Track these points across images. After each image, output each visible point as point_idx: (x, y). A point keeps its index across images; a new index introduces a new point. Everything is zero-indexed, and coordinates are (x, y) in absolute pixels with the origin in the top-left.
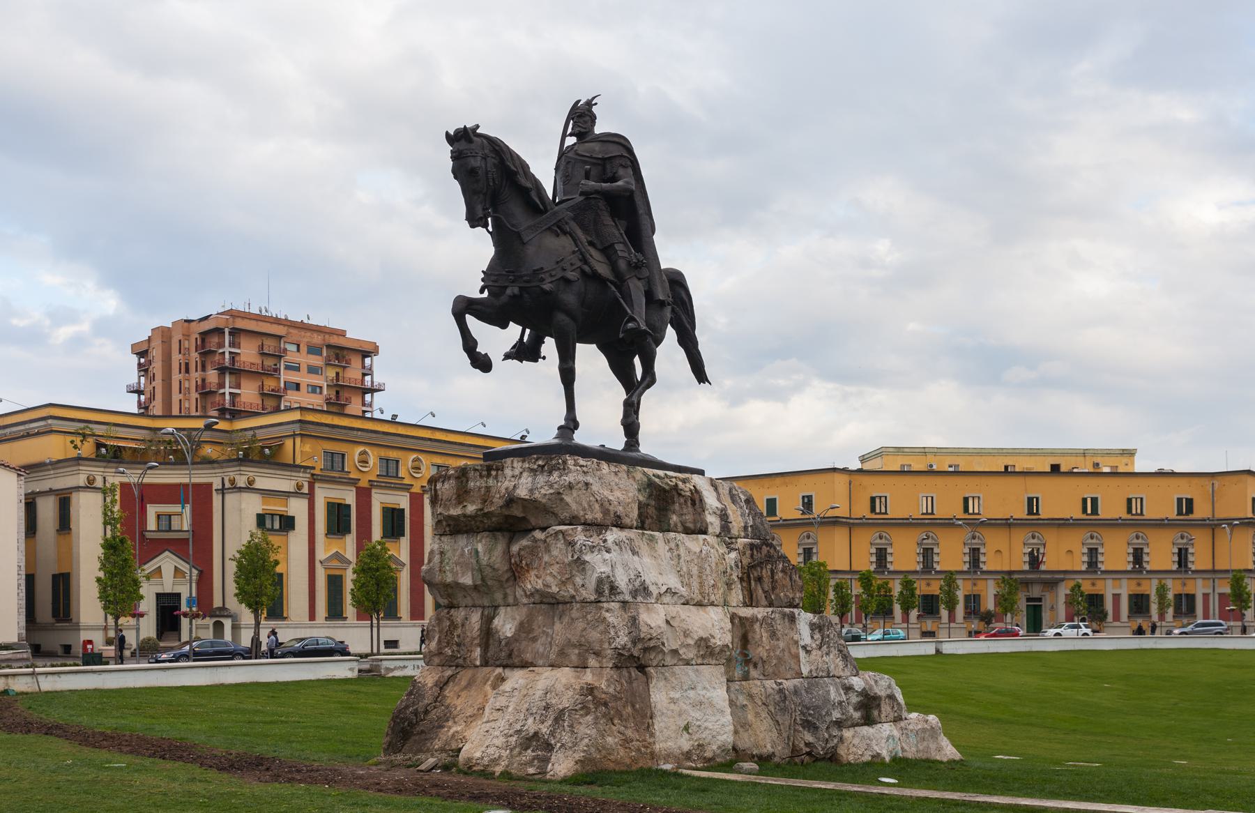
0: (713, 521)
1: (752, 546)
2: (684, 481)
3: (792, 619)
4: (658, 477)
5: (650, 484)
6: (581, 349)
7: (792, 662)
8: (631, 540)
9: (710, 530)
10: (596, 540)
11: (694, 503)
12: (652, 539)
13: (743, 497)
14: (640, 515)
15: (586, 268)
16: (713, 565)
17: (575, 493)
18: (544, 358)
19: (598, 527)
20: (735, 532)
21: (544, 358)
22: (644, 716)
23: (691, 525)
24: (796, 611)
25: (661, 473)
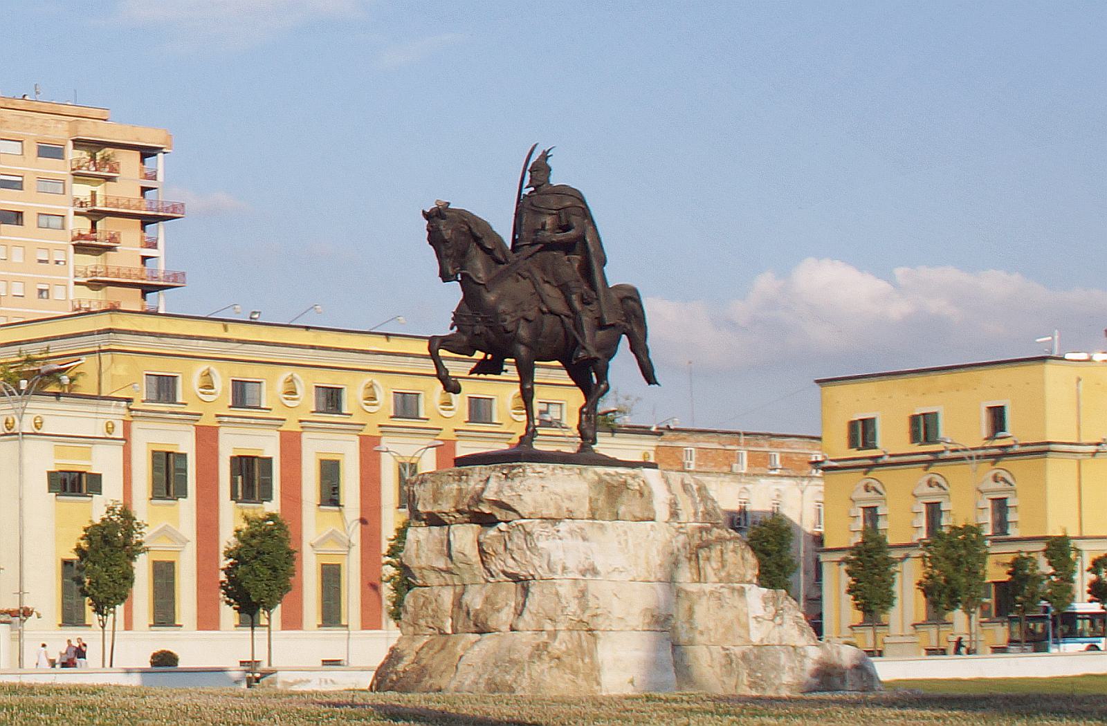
0: (662, 511)
1: (701, 529)
2: (634, 477)
3: (742, 592)
5: (601, 481)
6: (540, 374)
7: (742, 632)
8: (581, 529)
9: (657, 518)
11: (642, 495)
12: (602, 527)
13: (695, 487)
14: (591, 509)
19: (555, 520)
20: (683, 518)
22: (594, 673)
23: (639, 515)
24: (747, 586)
25: (611, 470)
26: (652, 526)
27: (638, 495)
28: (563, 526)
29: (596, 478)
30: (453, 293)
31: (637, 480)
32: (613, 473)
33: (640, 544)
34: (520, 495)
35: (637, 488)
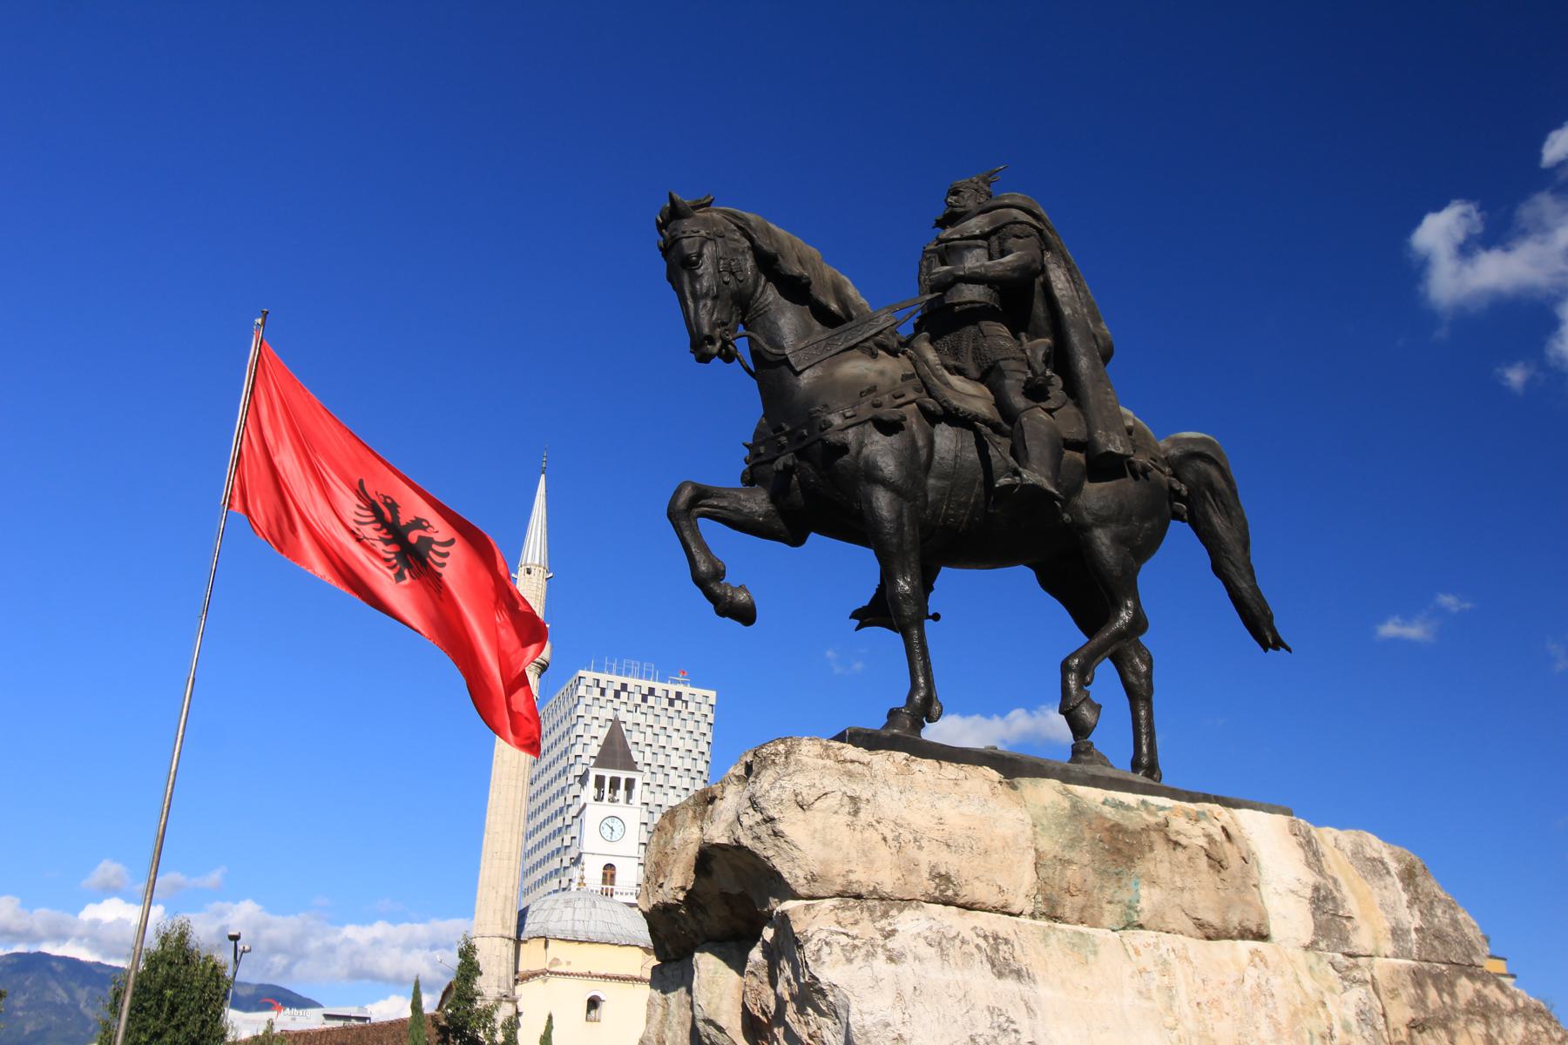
0: (1290, 919)
4: (1120, 805)
5: (1078, 811)
9: (1274, 929)
10: (867, 929)
11: (1217, 864)
14: (1043, 885)
15: (931, 404)
16: (1283, 1016)
17: (816, 817)
18: (936, 617)
19: (889, 902)
21: (936, 617)
23: (1212, 918)
26: (1254, 953)
27: (1203, 862)
28: (910, 924)
29: (1067, 804)
30: (736, 404)
31: (1204, 824)
32: (1134, 804)
33: (1214, 1003)
34: (772, 820)
35: (1203, 842)
